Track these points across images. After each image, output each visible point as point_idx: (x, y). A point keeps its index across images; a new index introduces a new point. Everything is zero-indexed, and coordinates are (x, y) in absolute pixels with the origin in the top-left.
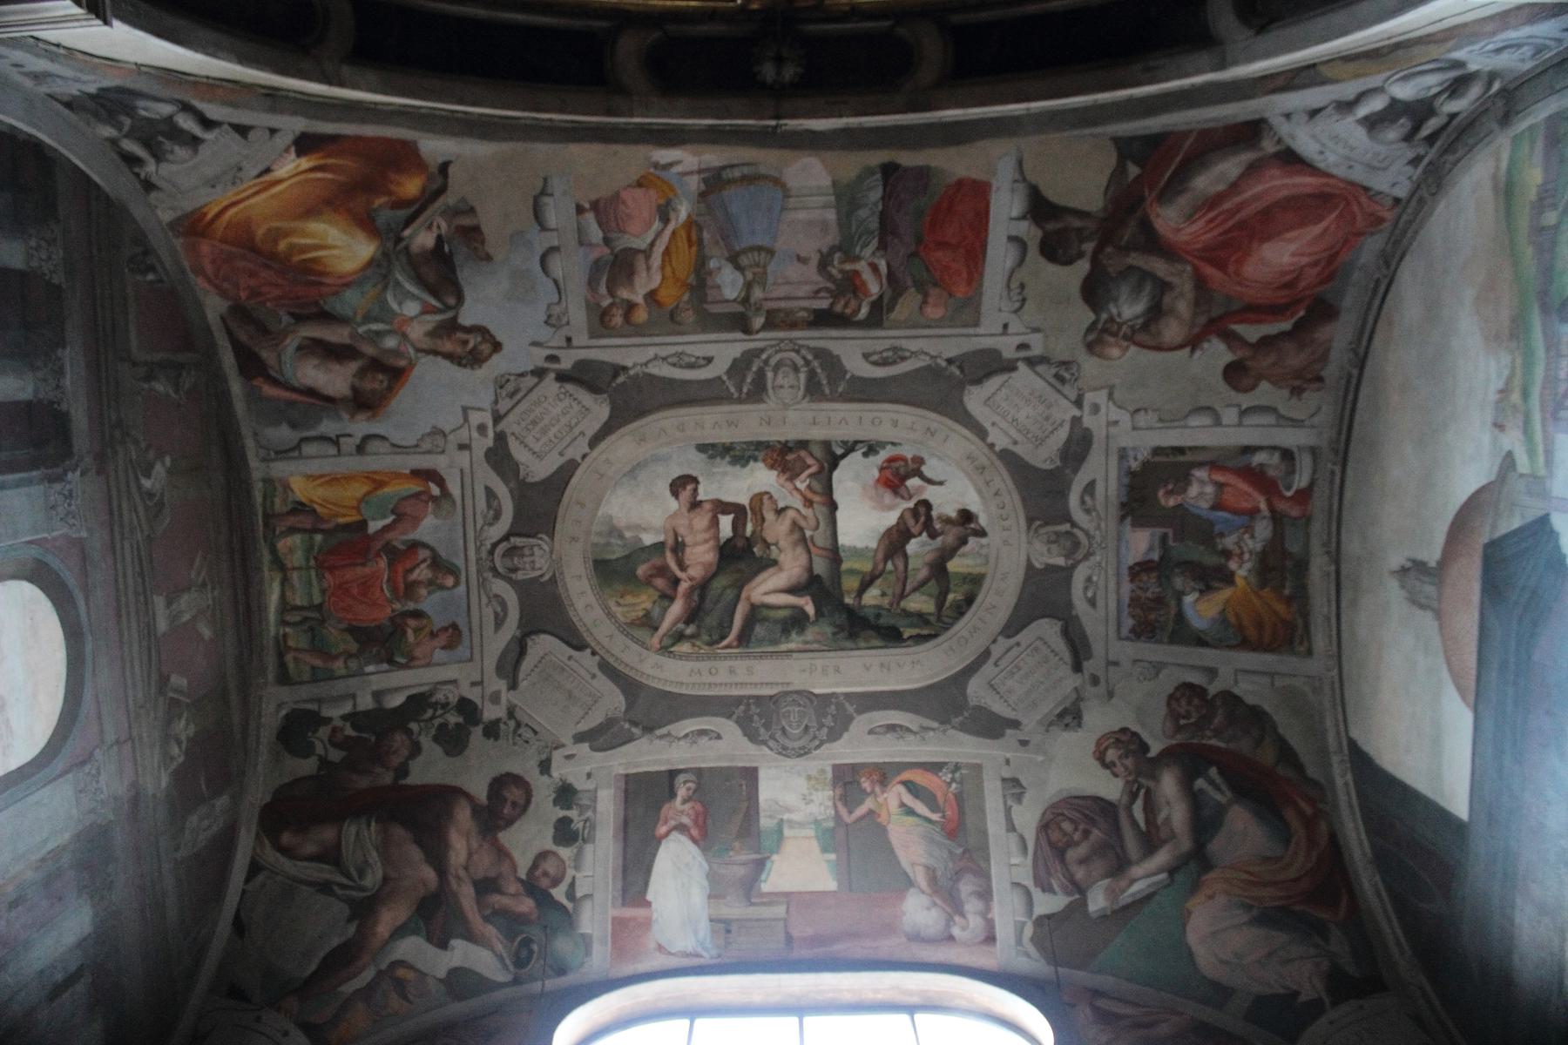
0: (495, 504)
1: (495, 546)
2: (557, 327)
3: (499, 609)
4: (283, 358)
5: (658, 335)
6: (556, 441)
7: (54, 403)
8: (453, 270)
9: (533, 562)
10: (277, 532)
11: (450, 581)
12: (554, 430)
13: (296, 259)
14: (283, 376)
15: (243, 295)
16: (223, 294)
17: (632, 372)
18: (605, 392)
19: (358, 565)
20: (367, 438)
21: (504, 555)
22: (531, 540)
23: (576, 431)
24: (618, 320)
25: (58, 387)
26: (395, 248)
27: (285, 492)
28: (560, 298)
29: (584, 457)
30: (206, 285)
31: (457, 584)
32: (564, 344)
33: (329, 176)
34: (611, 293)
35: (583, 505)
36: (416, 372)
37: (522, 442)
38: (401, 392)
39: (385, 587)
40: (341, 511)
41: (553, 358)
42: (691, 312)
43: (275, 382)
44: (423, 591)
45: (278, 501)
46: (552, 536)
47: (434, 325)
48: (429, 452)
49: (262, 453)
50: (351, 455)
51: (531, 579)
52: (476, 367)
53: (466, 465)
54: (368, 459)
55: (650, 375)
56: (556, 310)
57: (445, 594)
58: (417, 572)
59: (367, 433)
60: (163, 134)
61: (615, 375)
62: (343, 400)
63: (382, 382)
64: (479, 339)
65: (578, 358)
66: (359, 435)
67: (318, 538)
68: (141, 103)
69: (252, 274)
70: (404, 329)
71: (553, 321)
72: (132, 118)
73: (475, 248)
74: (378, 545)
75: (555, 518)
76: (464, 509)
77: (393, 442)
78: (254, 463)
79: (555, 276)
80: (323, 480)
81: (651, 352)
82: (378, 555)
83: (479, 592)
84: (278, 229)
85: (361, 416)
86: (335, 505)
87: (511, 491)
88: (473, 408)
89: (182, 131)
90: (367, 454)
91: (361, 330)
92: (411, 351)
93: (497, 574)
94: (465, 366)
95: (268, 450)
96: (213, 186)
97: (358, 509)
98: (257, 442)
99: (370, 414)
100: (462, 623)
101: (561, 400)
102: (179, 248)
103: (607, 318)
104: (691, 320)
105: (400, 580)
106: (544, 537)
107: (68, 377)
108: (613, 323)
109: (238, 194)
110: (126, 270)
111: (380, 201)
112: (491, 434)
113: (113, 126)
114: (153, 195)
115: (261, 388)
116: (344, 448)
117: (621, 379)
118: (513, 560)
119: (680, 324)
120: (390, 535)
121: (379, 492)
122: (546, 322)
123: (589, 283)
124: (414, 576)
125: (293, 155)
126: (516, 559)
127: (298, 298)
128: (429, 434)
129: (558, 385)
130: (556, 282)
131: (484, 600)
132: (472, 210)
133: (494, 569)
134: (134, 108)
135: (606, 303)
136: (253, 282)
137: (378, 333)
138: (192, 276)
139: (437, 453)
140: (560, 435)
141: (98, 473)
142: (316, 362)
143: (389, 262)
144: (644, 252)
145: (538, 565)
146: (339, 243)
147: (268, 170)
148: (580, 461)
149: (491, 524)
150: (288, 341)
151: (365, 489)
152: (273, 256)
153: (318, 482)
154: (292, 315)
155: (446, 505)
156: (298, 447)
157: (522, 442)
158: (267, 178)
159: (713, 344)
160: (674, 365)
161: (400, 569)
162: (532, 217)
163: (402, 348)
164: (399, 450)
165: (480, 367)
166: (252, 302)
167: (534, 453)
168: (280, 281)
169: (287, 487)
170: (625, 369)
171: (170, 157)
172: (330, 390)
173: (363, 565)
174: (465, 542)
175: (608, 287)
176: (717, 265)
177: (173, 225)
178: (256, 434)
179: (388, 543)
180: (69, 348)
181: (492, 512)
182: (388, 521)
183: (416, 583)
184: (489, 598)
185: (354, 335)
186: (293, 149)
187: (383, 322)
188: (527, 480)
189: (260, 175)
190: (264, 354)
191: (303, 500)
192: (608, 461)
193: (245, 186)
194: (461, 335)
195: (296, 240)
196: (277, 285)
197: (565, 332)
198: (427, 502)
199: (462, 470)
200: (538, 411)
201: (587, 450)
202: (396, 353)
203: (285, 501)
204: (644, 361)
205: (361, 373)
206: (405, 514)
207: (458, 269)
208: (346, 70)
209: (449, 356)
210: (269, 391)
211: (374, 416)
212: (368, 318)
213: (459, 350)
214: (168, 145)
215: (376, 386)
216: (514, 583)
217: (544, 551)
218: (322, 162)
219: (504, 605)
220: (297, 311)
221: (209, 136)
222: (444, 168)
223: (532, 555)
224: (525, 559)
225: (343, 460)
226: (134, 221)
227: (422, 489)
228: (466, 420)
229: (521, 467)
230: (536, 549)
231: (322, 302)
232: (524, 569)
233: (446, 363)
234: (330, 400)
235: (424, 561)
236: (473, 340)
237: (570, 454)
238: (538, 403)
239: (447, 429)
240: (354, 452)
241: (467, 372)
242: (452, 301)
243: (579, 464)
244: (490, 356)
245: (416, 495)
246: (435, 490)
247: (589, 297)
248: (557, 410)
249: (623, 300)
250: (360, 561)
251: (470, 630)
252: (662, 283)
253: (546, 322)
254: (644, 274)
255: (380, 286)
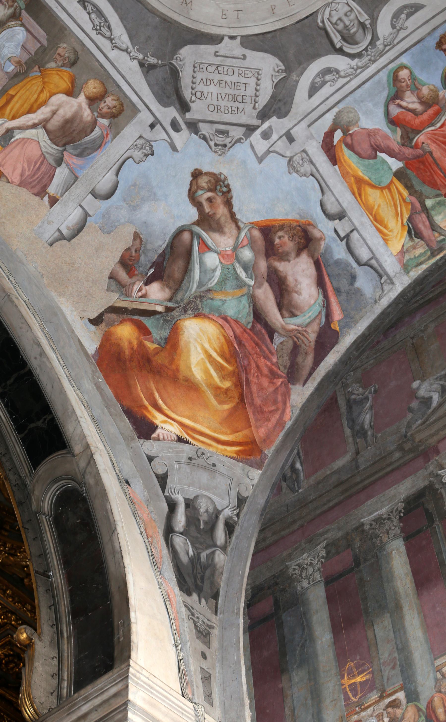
0: (318, 80)
1: (352, 56)
2: (149, 143)
3: (403, 16)
4: (308, 320)
5: (98, 61)
6: (236, 70)
7: (400, 517)
8: (163, 255)
9: (346, 15)
10: (442, 237)
11: (404, 74)
12: (229, 79)
13: (230, 368)
14: (320, 313)
15: (279, 382)
16: (287, 395)
17: (141, 56)
18: (171, 64)
19: (433, 158)
20: (330, 217)
21: (356, 43)
22: (329, 29)
23: (218, 60)
24: (110, 101)
25: (389, 519)
26: (176, 308)
27: (407, 251)
28: (129, 158)
29: (232, 38)
30: (288, 410)
31: (402, 67)
32: (158, 126)
33: (157, 395)
34: (94, 123)
35: (273, 8)
36: (257, 218)
37: (256, 96)
38: (280, 218)
39: (439, 125)
40: (397, 197)
41: (175, 126)
42: (60, 51)
43: (329, 315)
44: (425, 91)
45: (418, 252)
46: (315, 14)
47: (211, 233)
48: (311, 162)
49: (386, 288)
50: (350, 220)
51: (361, 7)
52: (222, 177)
53: (304, 124)
54: (345, 205)
55: (131, 38)
56: (138, 154)
57: (417, 73)
58: (411, 106)
59: (326, 220)
60: (198, 527)
61: (152, 67)
62: (312, 256)
63: (280, 238)
64: (200, 192)
65: (161, 107)
66: (331, 224)
67: (429, 203)
68: (184, 559)
69: (261, 389)
70: (230, 253)
71: (147, 150)
72: (199, 554)
73: (136, 251)
74: (408, 151)
75: (297, 22)
76: (338, 102)
77: (320, 193)
78: (399, 288)
79: (114, 177)
80: (381, 228)
81: (113, 54)
82: (416, 146)
83: (398, 43)
84: (216, 396)
85: (316, 233)
86: (395, 205)
87: (302, 73)
88: (256, 154)
89: (188, 518)
90: (342, 208)
91: (252, 283)
92: (243, 234)
93: (375, 38)
94: (228, 186)
95: (382, 284)
96: (214, 465)
97: (388, 187)
98: (380, 298)
99: (310, 228)
100: (432, 42)
101: (202, 93)
102: (273, 448)
103: (114, 110)
104: (65, 45)
105: (425, 116)
106: (319, 21)
107: (379, 512)
108: (115, 103)
109: (210, 445)
110: (300, 491)
111: (151, 346)
112: (266, 125)
113: (213, 559)
114: (245, 494)
115: (339, 321)
116: (348, 230)
117: (152, 60)
118: (355, 33)
119: (75, 51)
120: (396, 147)
121: (366, 178)
122: (152, 154)
123: (100, 147)
124: (417, 106)
125: (159, 431)
126: (352, 31)
127: (257, 344)
128: (297, 172)
129: (192, 105)
130: (117, 174)
131: (402, 34)
132: (112, 277)
133: (372, 43)
134: (191, 560)
135: (105, 122)
136: (265, 382)
137: (245, 268)
138: (288, 424)
139: (308, 155)
140: (230, 71)
141: (437, 452)
142: (295, 296)
143: (189, 303)
144: (44, 127)
145: (347, 8)
146: (199, 349)
147: (180, 440)
148: (239, 38)
149: (337, 72)
150: (293, 327)
151: (369, 190)
152: (239, 384)
153: (385, 231)
154: (272, 339)
155: (345, 119)
156: (367, 264)
157: (256, 96)
158: (185, 436)
159: (70, 11)
160: (109, 27)
161: (417, 121)
162: (85, 229)
163: (245, 242)
164: (323, 185)
165: (221, 174)
166: (280, 373)
167: (258, 79)
168: (253, 365)
169: (403, 252)
170: (141, 64)
171: (211, 510)
172: (312, 271)
173: (431, 153)
174: (364, 83)
175: (92, 131)
176: (8, 63)
177: (259, 466)
178: (376, 302)
179: (403, 145)
180: (362, 520)
181: (327, 78)
182: (384, 156)
183: (422, 102)
184: (399, 31)
185: (259, 285)
186: (154, 436)
187: (235, 270)
188: (283, 68)
189: (187, 442)
190: (312, 337)
191: (406, 233)
192: (224, 16)
193: (200, 445)
194: (207, 209)
195: (217, 380)
196: (258, 366)
197: (148, 134)
198: (351, 135)
199: (309, 126)
200: (223, 103)
201: (226, 39)
202: (252, 244)
203: (414, 248)
204: (124, 54)
205: (284, 257)
206: (372, 146)
207: (160, 251)
208: (77, 449)
209: (229, 204)
210: (337, 314)
211: (310, 224)
212: (241, 285)
213: (219, 200)
214: (204, 517)
215: (286, 239)
216: (374, 20)
217: (330, 10)
218: (150, 408)
219: (396, 16)
220: (267, 337)
221: (180, 499)
222: (96, 322)
223: (340, 19)
224: (347, 23)
225: (357, 224)
226: (267, 502)
227: (343, 146)
228: (268, 152)
229: (276, 81)
230: (334, 20)
231: (250, 326)
232: (357, 16)
233: (235, 203)
234: (317, 264)
235: (400, 106)
236: (203, 196)
237: (239, 51)
238: (218, 109)
239: (284, 161)
240: (346, 218)
241: (230, 181)
242: (186, 236)
243: (242, 37)
244: (206, 174)
245: (351, 147)
246: (338, 135)
247: (110, 136)
248: (213, 89)
249: (92, 111)
250: (430, 159)
251: (435, 29)
252: (55, 94)
253: (152, 154)
254: (61, 112)
255: (210, 295)
